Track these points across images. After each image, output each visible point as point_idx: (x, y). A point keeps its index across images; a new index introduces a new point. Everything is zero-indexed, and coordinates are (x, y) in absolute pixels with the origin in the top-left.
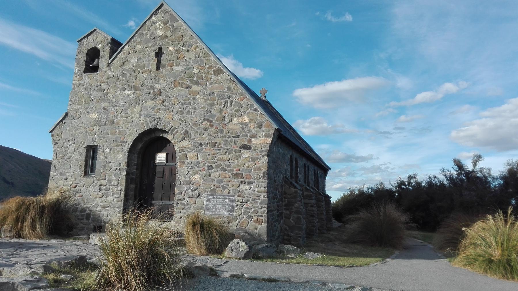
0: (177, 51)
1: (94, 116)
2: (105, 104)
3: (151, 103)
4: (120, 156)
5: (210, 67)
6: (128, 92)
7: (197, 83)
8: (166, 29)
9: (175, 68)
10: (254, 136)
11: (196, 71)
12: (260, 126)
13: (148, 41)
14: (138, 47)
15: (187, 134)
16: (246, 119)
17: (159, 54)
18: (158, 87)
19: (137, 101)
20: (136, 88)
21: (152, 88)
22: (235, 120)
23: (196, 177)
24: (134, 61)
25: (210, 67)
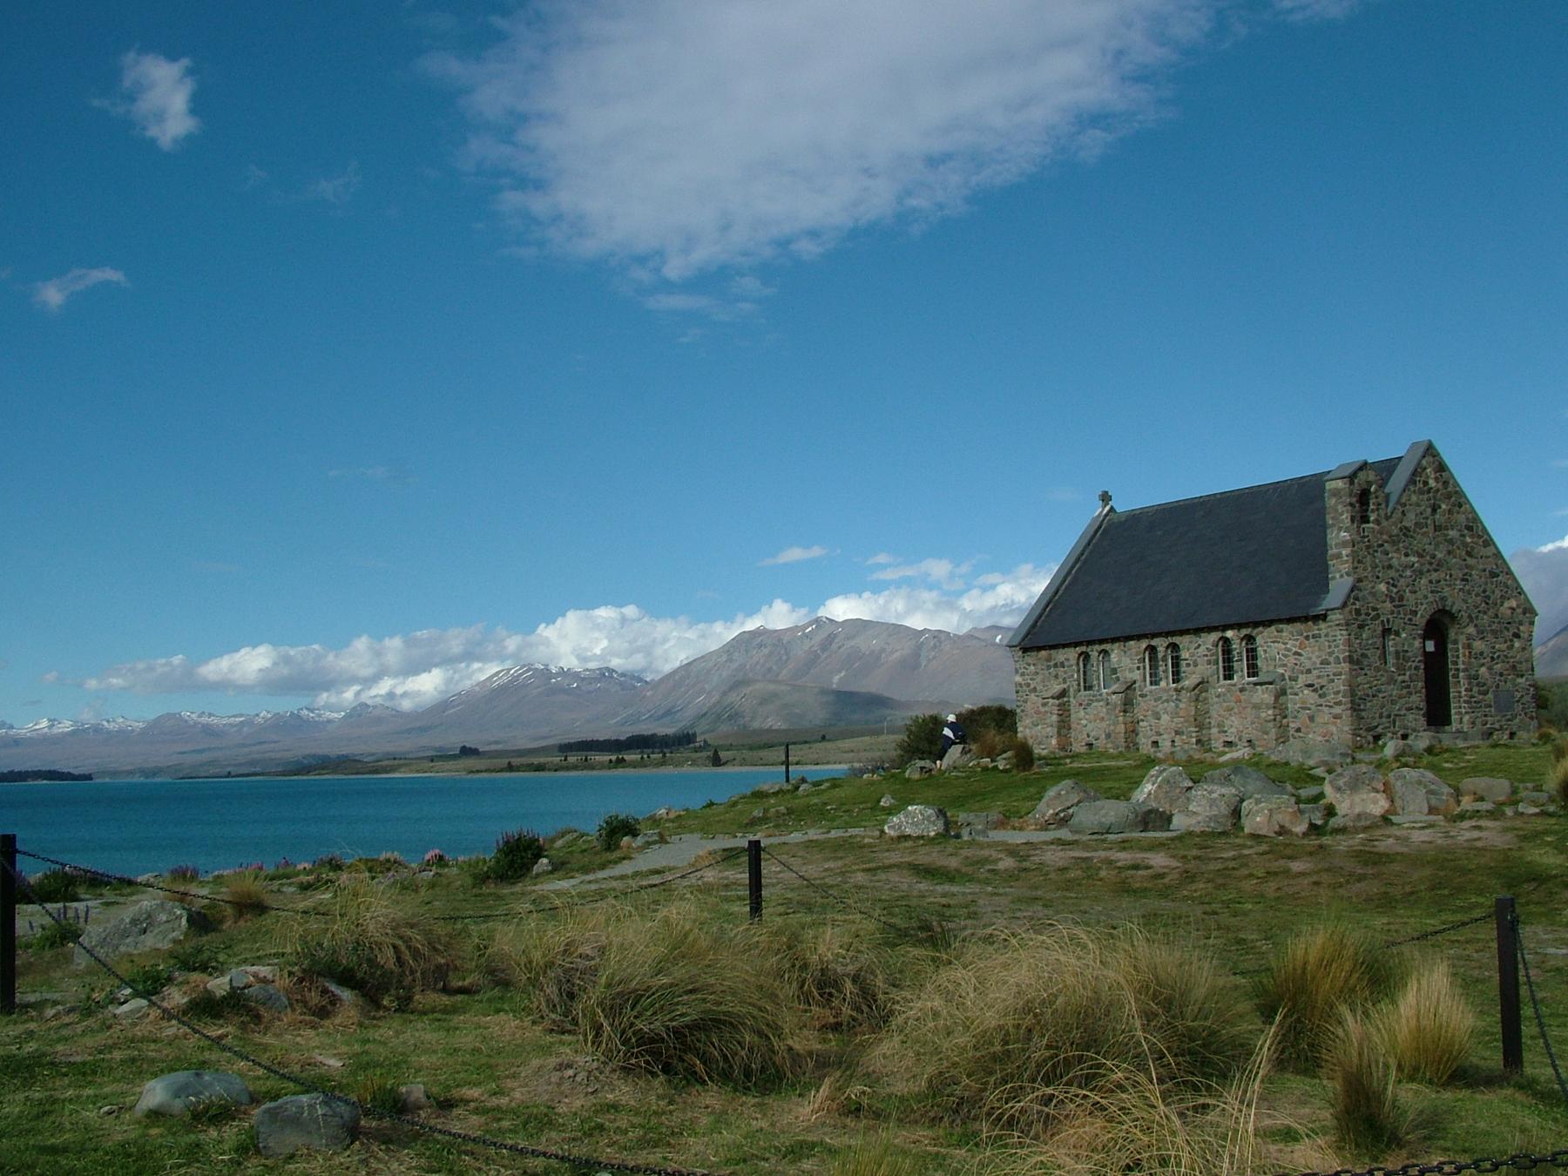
0: (1450, 512)
2: (1392, 573)
3: (1434, 576)
5: (1480, 537)
6: (1414, 559)
7: (1469, 554)
8: (1436, 479)
9: (1451, 533)
10: (1521, 623)
11: (1468, 540)
13: (1421, 492)
14: (1414, 498)
16: (1513, 603)
17: (1434, 511)
18: (1439, 555)
19: (1421, 573)
21: (1434, 557)
23: (1483, 669)
25: (1480, 537)
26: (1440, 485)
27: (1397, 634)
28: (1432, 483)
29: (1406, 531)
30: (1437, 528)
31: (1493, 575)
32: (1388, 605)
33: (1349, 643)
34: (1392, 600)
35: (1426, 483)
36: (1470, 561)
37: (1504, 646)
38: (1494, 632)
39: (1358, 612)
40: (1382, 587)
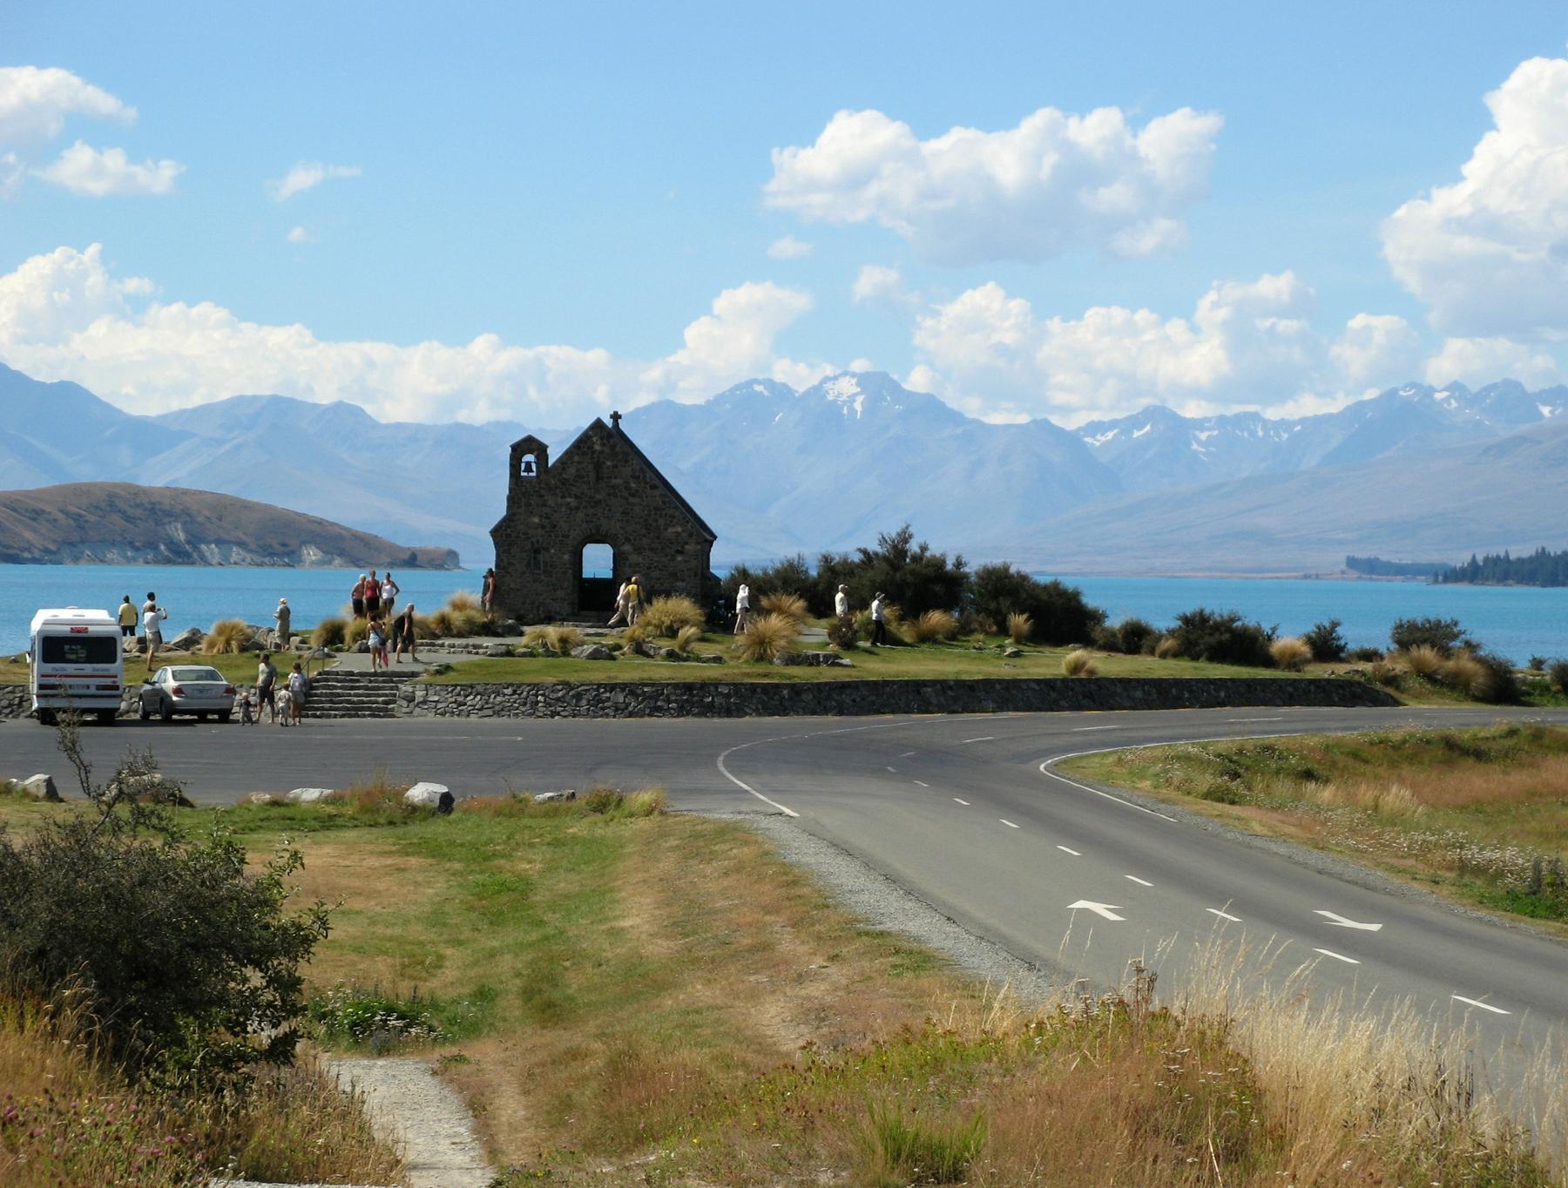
0: (615, 466)
1: (536, 520)
3: (591, 511)
4: (566, 557)
8: (603, 445)
12: (691, 535)
13: (585, 454)
14: (576, 458)
15: (628, 540)
19: (577, 508)
20: (576, 497)
22: (670, 530)
24: (572, 470)
26: (607, 450)
27: (547, 550)
28: (597, 447)
29: (564, 482)
30: (599, 478)
31: (656, 509)
32: (540, 531)
33: (498, 555)
34: (543, 527)
35: (590, 447)
36: (632, 500)
37: (665, 560)
38: (651, 549)
39: (508, 536)
40: (536, 520)
